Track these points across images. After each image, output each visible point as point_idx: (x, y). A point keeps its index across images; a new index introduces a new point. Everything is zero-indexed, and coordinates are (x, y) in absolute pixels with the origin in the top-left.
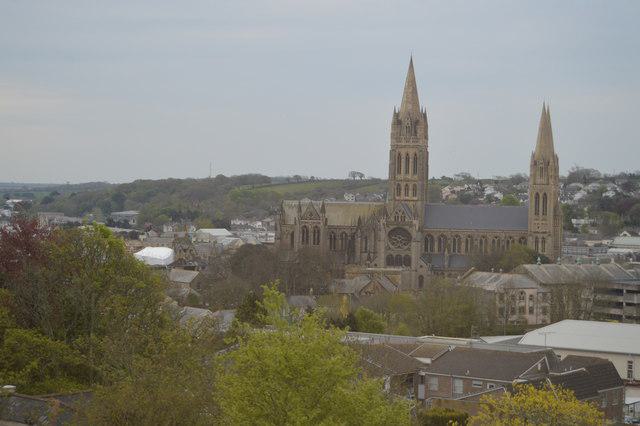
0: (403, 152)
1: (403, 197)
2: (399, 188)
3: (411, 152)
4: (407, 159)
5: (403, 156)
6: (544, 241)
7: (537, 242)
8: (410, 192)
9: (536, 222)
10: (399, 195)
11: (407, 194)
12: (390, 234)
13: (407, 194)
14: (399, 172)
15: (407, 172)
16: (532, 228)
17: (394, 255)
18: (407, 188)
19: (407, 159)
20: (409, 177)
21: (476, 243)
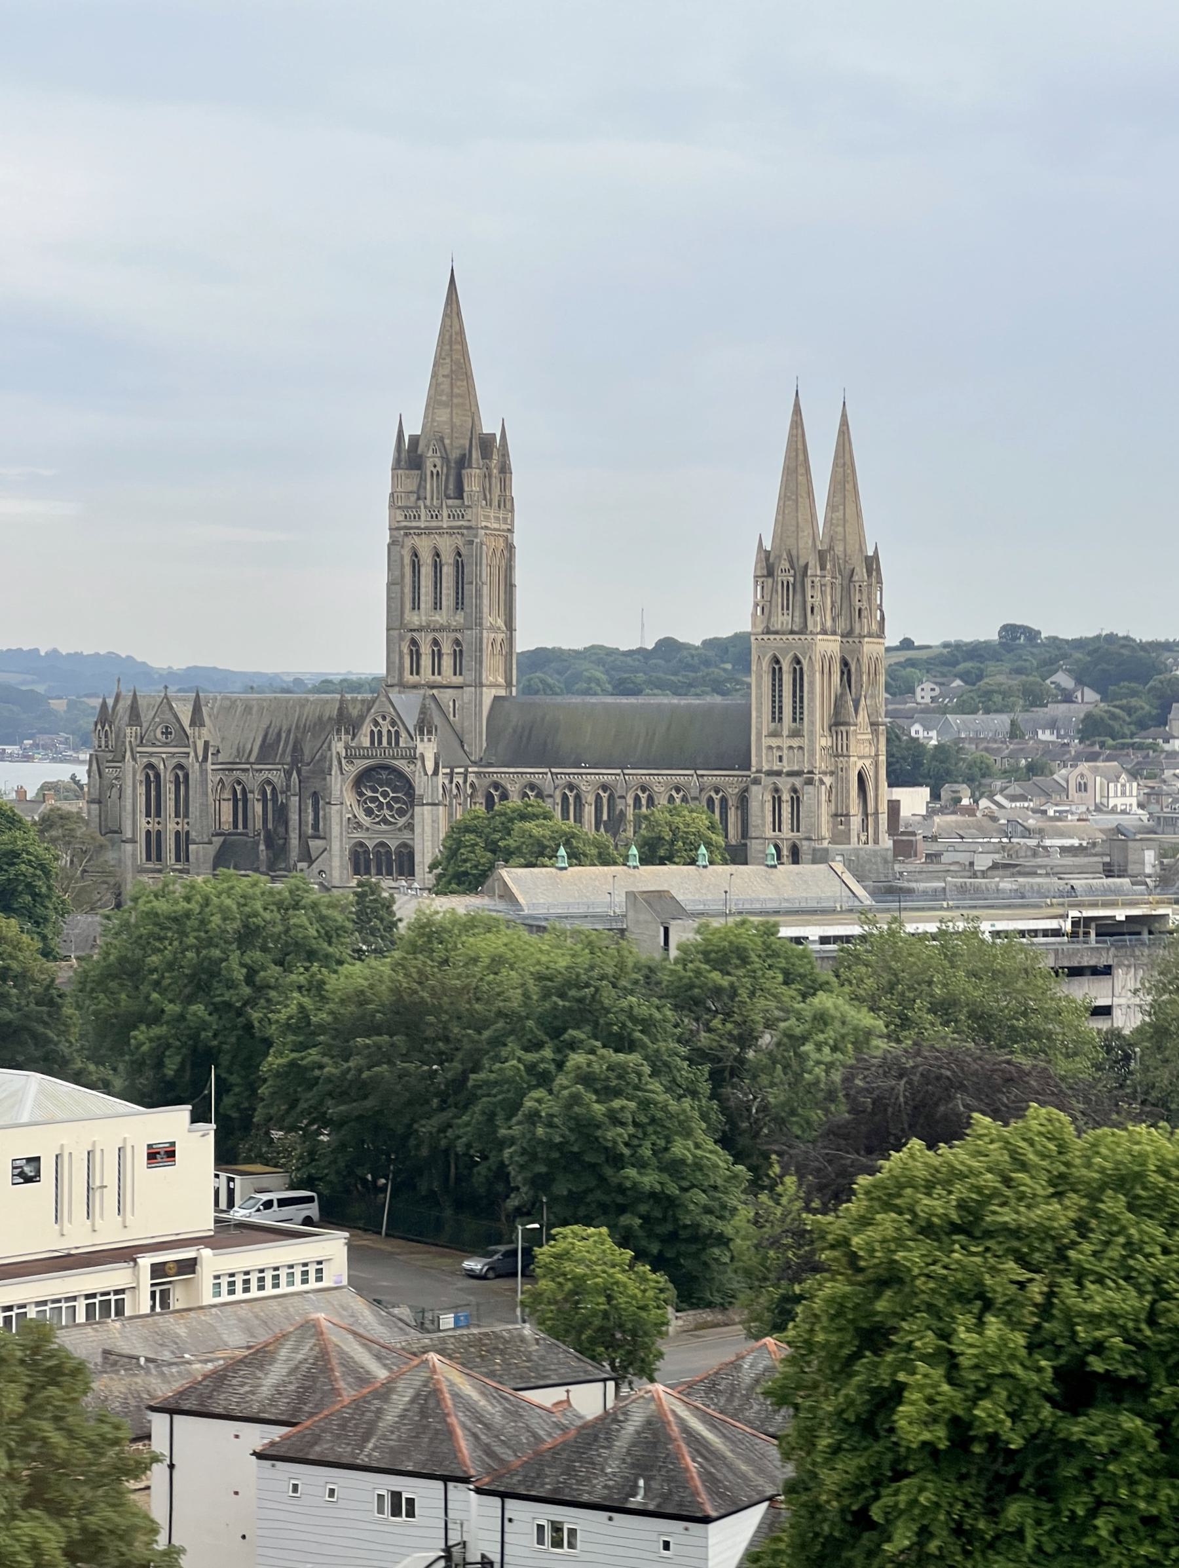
0: (424, 546)
1: (426, 675)
2: (416, 655)
3: (446, 546)
4: (437, 567)
5: (426, 558)
6: (796, 802)
7: (777, 801)
8: (447, 662)
9: (774, 742)
10: (416, 669)
11: (437, 669)
12: (360, 781)
13: (437, 669)
14: (416, 605)
15: (437, 605)
16: (761, 760)
17: (370, 845)
18: (437, 655)
19: (437, 567)
20: (440, 618)
21: (620, 805)
